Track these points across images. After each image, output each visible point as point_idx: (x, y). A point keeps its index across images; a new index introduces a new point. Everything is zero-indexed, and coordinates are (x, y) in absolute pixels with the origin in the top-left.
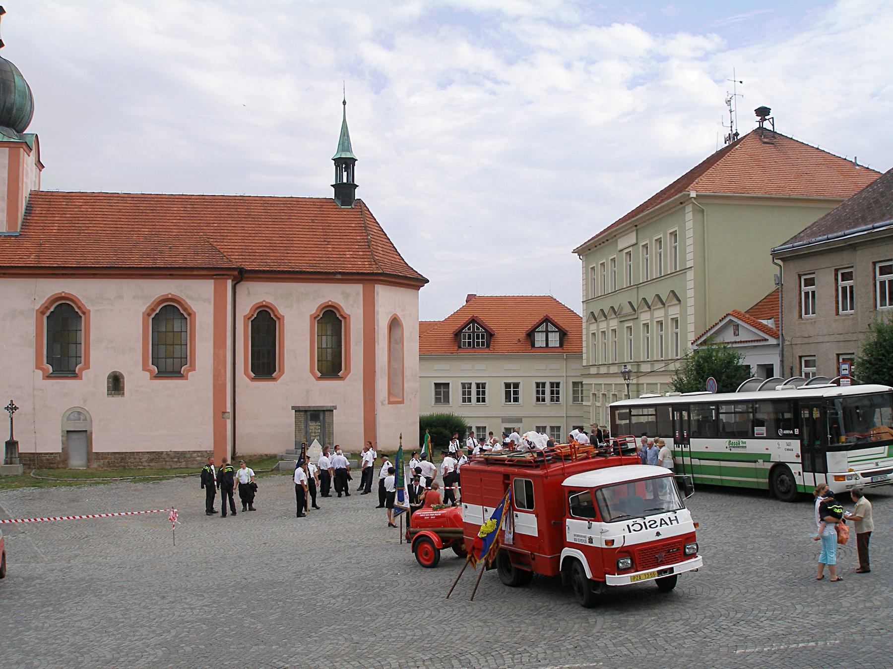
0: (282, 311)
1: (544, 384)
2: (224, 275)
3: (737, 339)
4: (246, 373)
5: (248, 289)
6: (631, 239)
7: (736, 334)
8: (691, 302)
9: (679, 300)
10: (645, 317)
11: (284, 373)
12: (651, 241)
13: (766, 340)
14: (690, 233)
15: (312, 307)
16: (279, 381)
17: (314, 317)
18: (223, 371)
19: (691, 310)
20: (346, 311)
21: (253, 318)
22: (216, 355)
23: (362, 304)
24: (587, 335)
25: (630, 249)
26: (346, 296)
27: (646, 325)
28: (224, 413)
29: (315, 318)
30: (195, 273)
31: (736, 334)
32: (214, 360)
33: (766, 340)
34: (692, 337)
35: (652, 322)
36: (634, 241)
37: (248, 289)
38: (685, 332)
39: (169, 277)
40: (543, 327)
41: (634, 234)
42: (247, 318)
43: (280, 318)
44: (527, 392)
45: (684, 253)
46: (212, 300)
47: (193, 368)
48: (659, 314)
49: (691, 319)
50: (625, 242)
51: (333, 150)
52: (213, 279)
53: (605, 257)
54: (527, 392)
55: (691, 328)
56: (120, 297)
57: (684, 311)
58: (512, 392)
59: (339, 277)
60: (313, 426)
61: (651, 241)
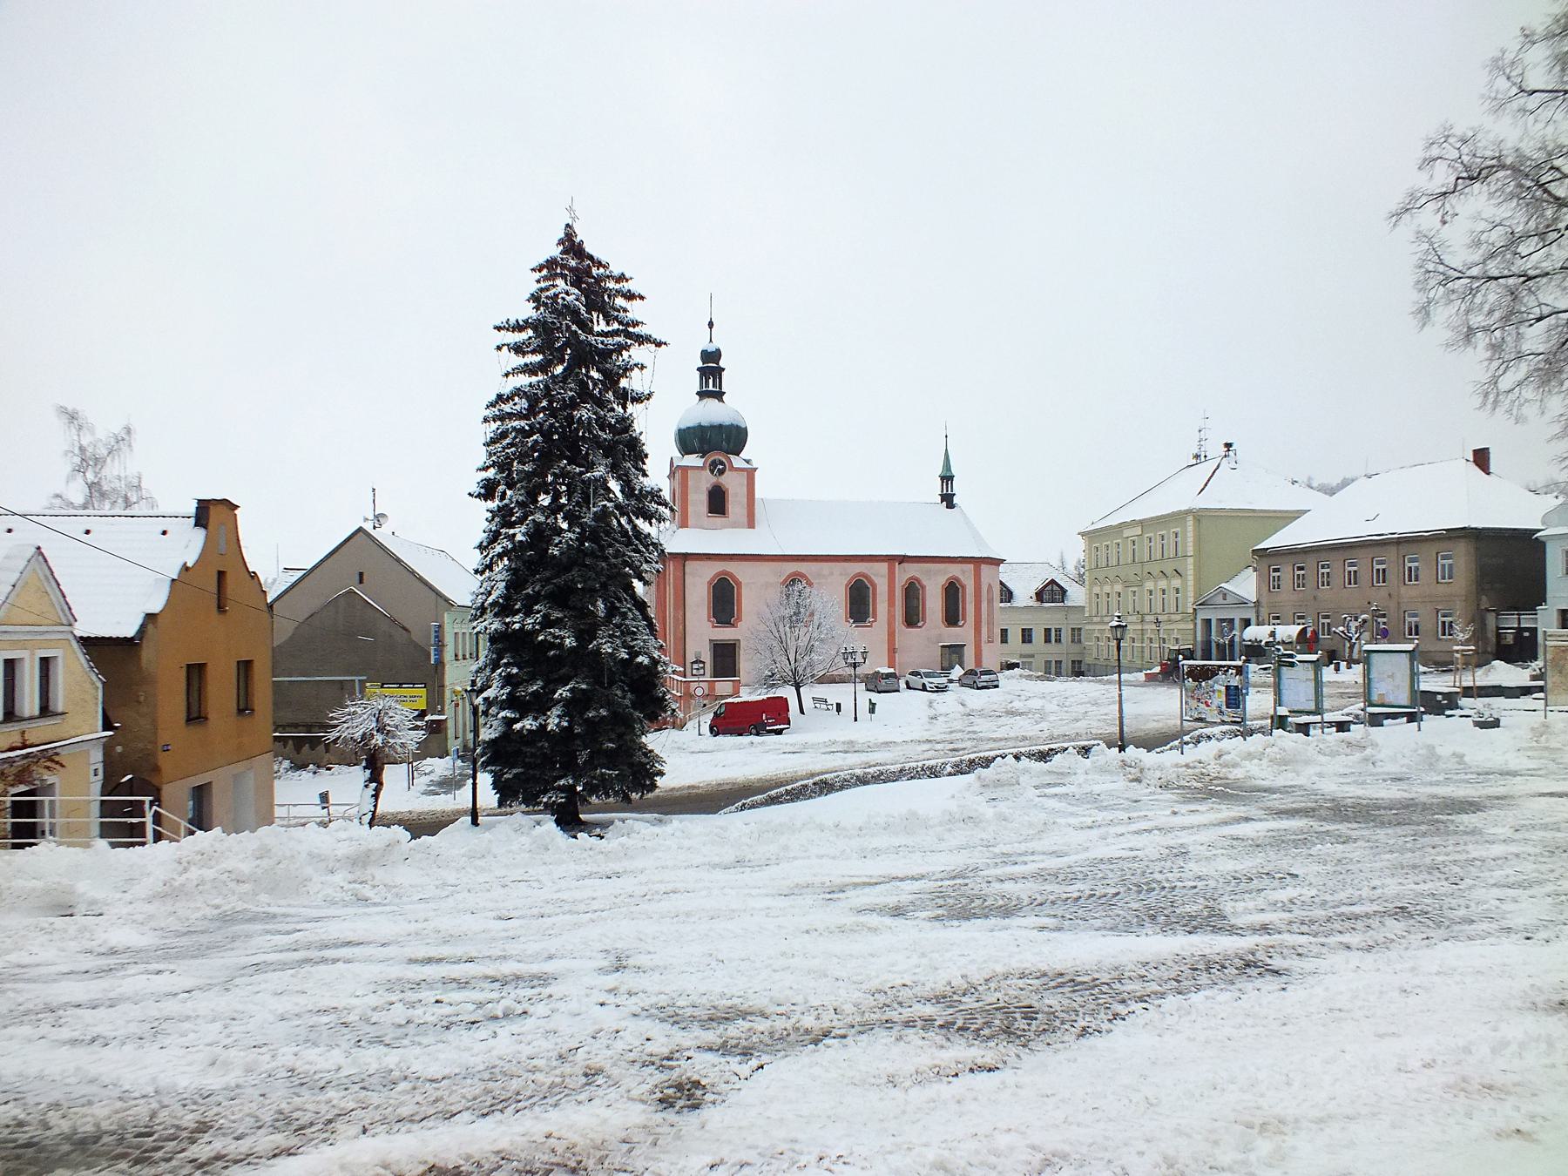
0: (924, 582)
1: (1050, 629)
8: (1191, 578)
10: (1149, 585)
12: (1155, 535)
14: (1190, 534)
15: (942, 580)
19: (1191, 583)
27: (1151, 592)
34: (1191, 600)
35: (1156, 588)
38: (1186, 597)
40: (1049, 588)
41: (1140, 528)
43: (923, 587)
44: (1038, 636)
45: (1185, 544)
48: (1163, 584)
49: (1191, 589)
51: (939, 470)
54: (1038, 636)
55: (1191, 594)
56: (832, 574)
57: (1185, 583)
58: (1027, 636)
60: (954, 657)
61: (1155, 535)
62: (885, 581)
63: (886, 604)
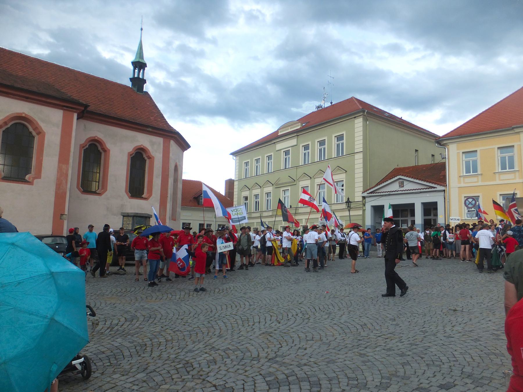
2: (72, 108)
3: (402, 189)
4: (78, 187)
5: (85, 126)
6: (293, 142)
7: (402, 185)
9: (346, 171)
11: (106, 190)
13: (434, 188)
15: (129, 147)
16: (103, 196)
17: (130, 154)
18: (64, 182)
20: (152, 154)
21: (85, 148)
22: (60, 169)
23: (162, 151)
24: (239, 198)
25: (290, 149)
26: (152, 144)
28: (62, 215)
29: (131, 155)
30: (49, 101)
31: (402, 185)
32: (58, 172)
33: (434, 188)
36: (295, 143)
37: (85, 126)
39: (25, 99)
42: (82, 146)
43: (106, 151)
46: (61, 126)
47: (38, 176)
50: (281, 146)
52: (62, 109)
53: (251, 158)
59: (150, 130)
62: (58, 131)
63: (56, 159)
